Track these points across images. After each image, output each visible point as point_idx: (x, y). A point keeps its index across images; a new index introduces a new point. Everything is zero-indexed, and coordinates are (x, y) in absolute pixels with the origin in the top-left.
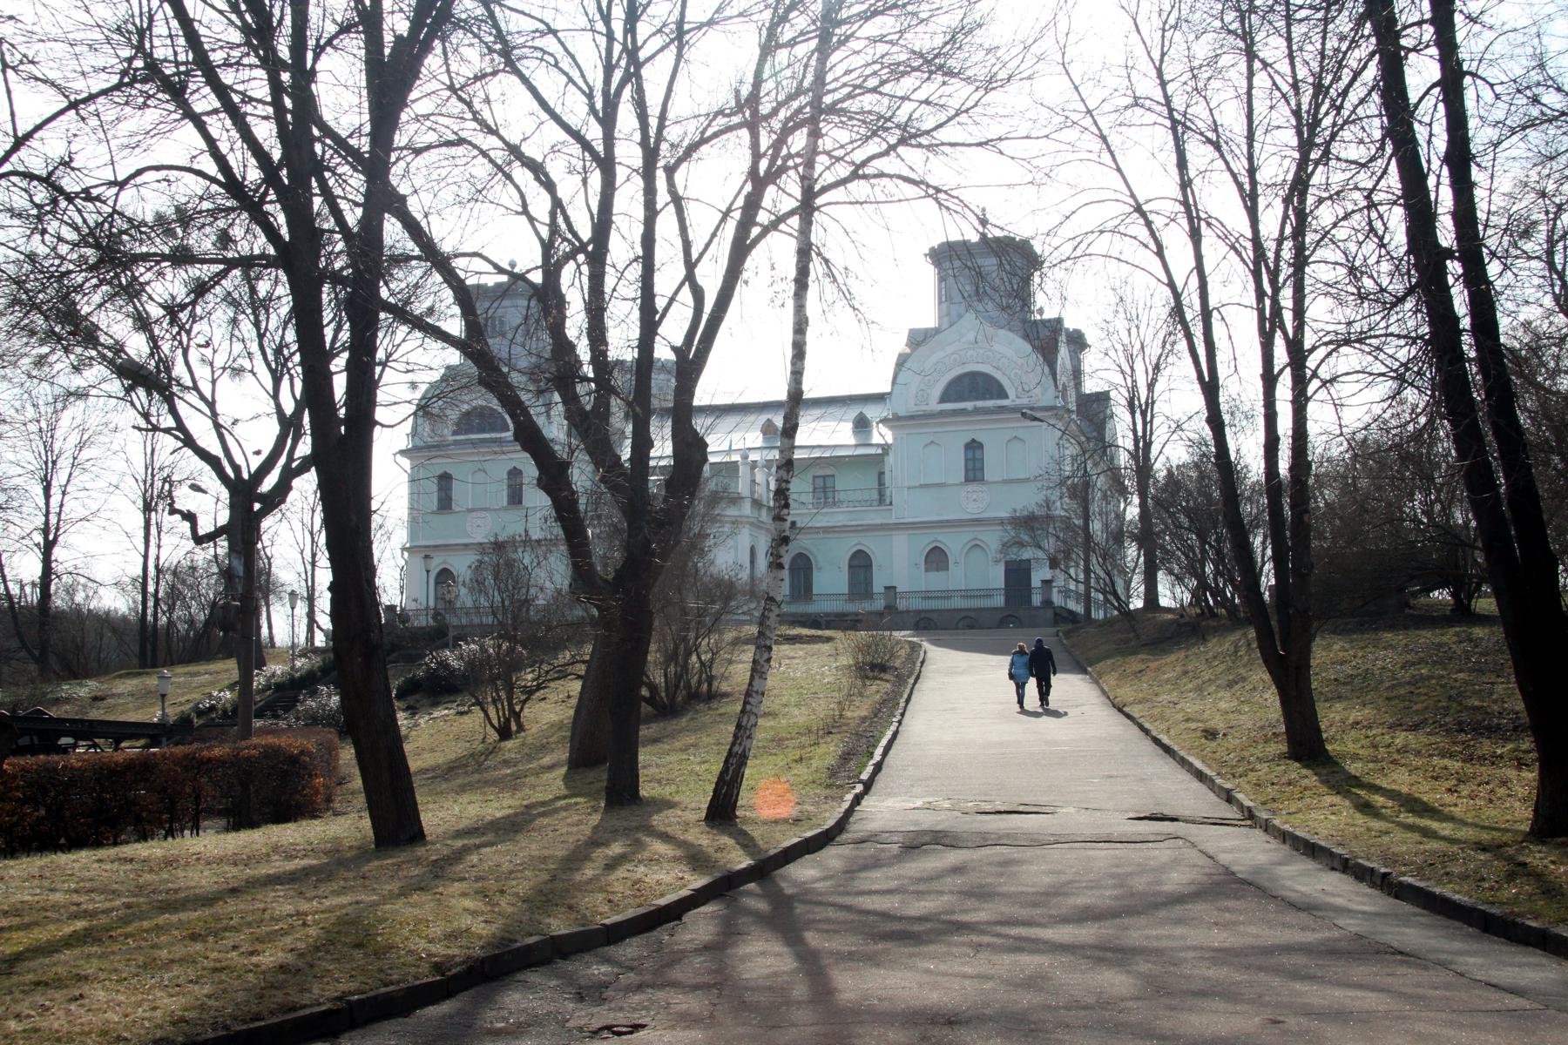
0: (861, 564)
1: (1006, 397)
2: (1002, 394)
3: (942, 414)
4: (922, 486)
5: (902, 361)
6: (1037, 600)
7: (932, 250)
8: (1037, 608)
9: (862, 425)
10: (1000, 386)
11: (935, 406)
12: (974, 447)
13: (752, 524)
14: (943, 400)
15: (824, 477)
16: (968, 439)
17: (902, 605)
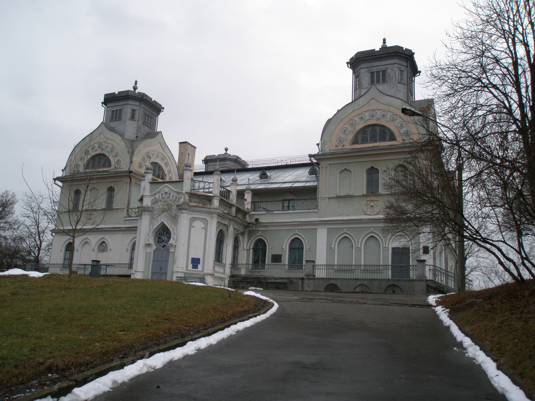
0: (296, 247)
2: (393, 138)
3: (353, 151)
4: (339, 197)
5: (329, 121)
6: (413, 275)
7: (351, 59)
8: (412, 280)
9: (312, 172)
11: (348, 146)
12: (372, 172)
13: (219, 215)
14: (355, 142)
15: (289, 200)
16: (369, 166)
17: (320, 273)
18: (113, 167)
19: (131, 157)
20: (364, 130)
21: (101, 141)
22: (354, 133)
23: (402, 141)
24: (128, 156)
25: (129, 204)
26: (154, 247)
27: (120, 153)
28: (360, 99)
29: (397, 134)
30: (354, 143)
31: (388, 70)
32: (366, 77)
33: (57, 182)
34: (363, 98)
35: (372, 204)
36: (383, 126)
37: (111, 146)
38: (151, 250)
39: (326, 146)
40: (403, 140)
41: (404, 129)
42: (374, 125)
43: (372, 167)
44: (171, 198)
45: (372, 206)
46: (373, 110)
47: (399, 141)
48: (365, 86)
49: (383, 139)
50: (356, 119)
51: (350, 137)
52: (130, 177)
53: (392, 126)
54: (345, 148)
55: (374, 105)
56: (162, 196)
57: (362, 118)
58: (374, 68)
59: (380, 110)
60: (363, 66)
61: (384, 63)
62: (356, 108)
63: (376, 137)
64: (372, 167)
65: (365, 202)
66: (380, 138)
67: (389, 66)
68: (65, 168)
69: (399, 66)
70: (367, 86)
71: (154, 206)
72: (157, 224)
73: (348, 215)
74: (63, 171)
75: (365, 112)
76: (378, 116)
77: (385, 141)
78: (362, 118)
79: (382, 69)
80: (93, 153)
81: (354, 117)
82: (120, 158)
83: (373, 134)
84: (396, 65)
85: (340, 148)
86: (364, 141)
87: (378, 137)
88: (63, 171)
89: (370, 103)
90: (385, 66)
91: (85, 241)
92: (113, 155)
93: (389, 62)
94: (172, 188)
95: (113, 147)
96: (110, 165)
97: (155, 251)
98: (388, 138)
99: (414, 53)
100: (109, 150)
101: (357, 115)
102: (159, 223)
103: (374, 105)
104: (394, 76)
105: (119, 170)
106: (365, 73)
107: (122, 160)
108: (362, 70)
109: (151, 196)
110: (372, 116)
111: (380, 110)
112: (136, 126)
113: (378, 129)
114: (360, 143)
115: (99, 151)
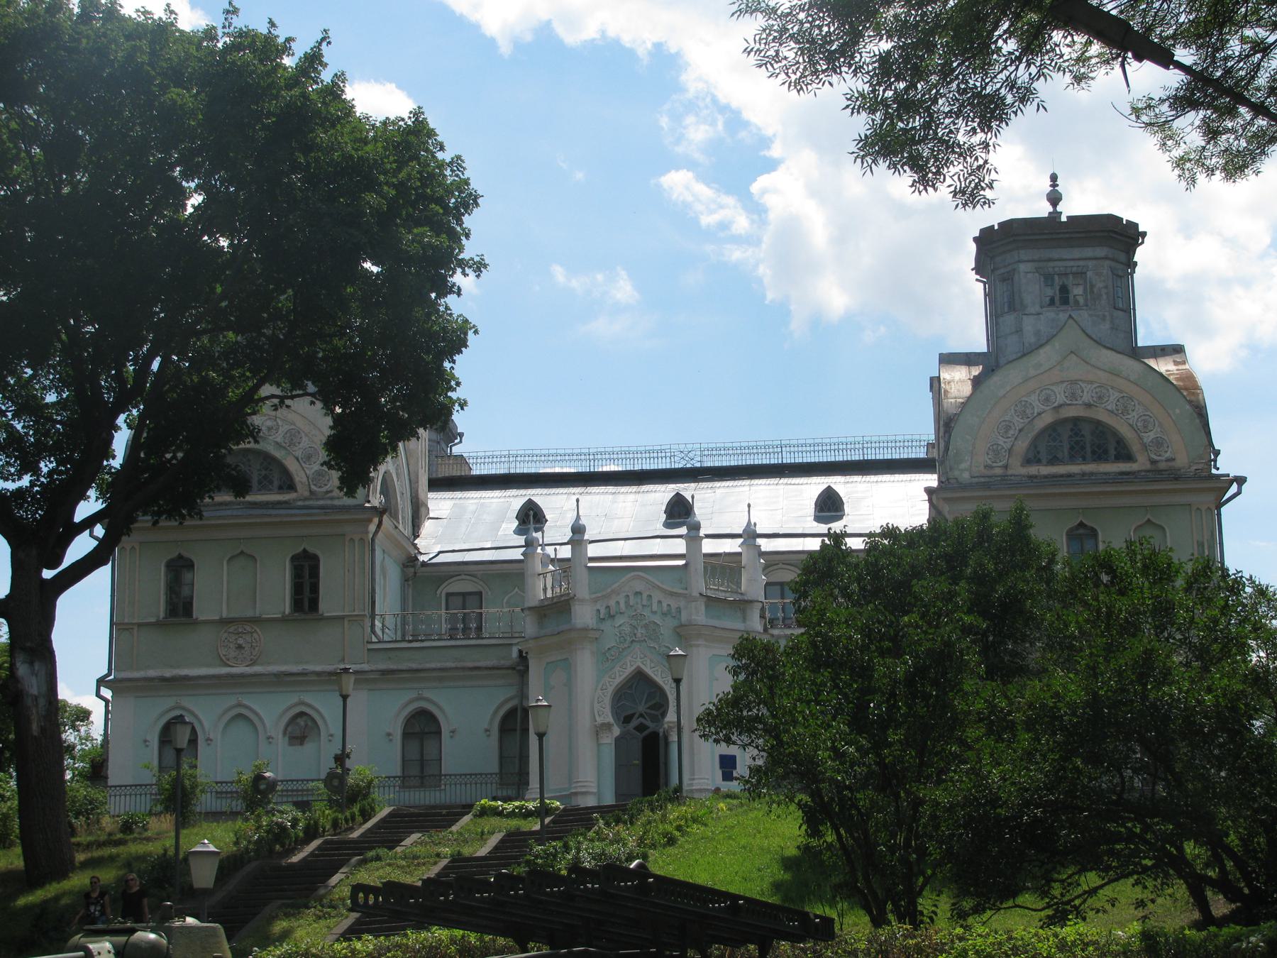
1: (1129, 458)
2: (1124, 454)
10: (1120, 442)
11: (1018, 470)
18: (302, 491)
20: (1053, 428)
22: (1031, 435)
23: (1148, 466)
26: (617, 731)
28: (1041, 351)
29: (1135, 448)
30: (1028, 462)
31: (1089, 274)
32: (1031, 288)
34: (1047, 348)
36: (1098, 423)
38: (608, 740)
39: (963, 466)
40: (1153, 462)
41: (1152, 435)
42: (1076, 421)
43: (1081, 525)
44: (655, 607)
48: (1031, 310)
49: (1100, 455)
50: (1033, 399)
51: (1022, 445)
54: (1010, 472)
56: (627, 603)
57: (1047, 399)
58: (1051, 264)
59: (1092, 383)
60: (1024, 254)
61: (1077, 253)
62: (1032, 372)
63: (1083, 448)
64: (1081, 525)
66: (1094, 452)
67: (1090, 263)
69: (1113, 264)
70: (1037, 308)
71: (607, 626)
72: (621, 674)
75: (1053, 384)
76: (1086, 398)
77: (1106, 461)
78: (1047, 399)
79: (1074, 269)
83: (1077, 443)
84: (1107, 263)
85: (998, 471)
86: (1053, 461)
87: (1089, 450)
90: (1081, 263)
91: (177, 713)
92: (299, 453)
93: (1088, 252)
94: (650, 578)
97: (617, 740)
98: (1112, 452)
99: (1144, 234)
100: (279, 440)
101: (1034, 392)
102: (630, 670)
104: (1104, 291)
105: (329, 502)
106: (1030, 276)
108: (1022, 267)
109: (595, 601)
110: (1073, 396)
111: (1092, 383)
113: (1086, 430)
114: (1044, 461)
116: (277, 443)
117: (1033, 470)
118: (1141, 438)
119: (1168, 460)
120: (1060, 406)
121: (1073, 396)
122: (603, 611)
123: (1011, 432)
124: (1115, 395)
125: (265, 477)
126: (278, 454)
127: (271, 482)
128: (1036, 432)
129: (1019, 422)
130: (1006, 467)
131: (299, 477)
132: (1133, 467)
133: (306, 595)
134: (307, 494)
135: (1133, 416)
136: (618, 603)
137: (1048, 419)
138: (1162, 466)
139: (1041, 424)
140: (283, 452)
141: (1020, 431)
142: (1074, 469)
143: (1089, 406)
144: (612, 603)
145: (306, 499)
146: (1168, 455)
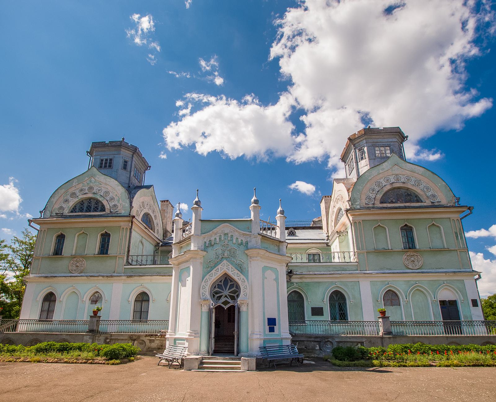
1: (422, 202)
2: (419, 200)
18: (107, 211)
19: (131, 203)
21: (92, 184)
23: (431, 204)
24: (128, 201)
25: (129, 251)
27: (116, 198)
33: (32, 224)
35: (412, 259)
37: (104, 190)
39: (357, 203)
40: (432, 203)
43: (406, 225)
45: (413, 261)
46: (396, 175)
47: (428, 203)
50: (382, 180)
51: (379, 196)
52: (132, 222)
53: (418, 190)
55: (397, 170)
59: (404, 175)
62: (381, 171)
64: (406, 225)
65: (406, 257)
68: (44, 209)
73: (390, 269)
74: (41, 212)
76: (403, 180)
80: (81, 197)
81: (380, 179)
82: (116, 203)
86: (392, 202)
88: (41, 212)
89: (394, 169)
95: (107, 193)
96: (104, 211)
100: (101, 194)
103: (397, 170)
107: (119, 205)
110: (398, 180)
112: (128, 176)
115: (90, 195)
116: (101, 195)
117: (385, 205)
118: (426, 194)
119: (438, 202)
120: (393, 183)
121: (398, 180)
122: (208, 243)
123: (374, 192)
124: (413, 179)
125: (96, 207)
126: (101, 199)
127: (98, 209)
128: (384, 192)
129: (377, 189)
130: (374, 204)
131: (107, 207)
132: (425, 204)
133: (104, 249)
134: (109, 212)
135: (422, 187)
136: (216, 239)
137: (388, 187)
138: (436, 204)
139: (386, 189)
140: (102, 198)
141: (378, 192)
142: (402, 205)
143: (404, 183)
144: (213, 239)
145: (108, 214)
146: (437, 200)
